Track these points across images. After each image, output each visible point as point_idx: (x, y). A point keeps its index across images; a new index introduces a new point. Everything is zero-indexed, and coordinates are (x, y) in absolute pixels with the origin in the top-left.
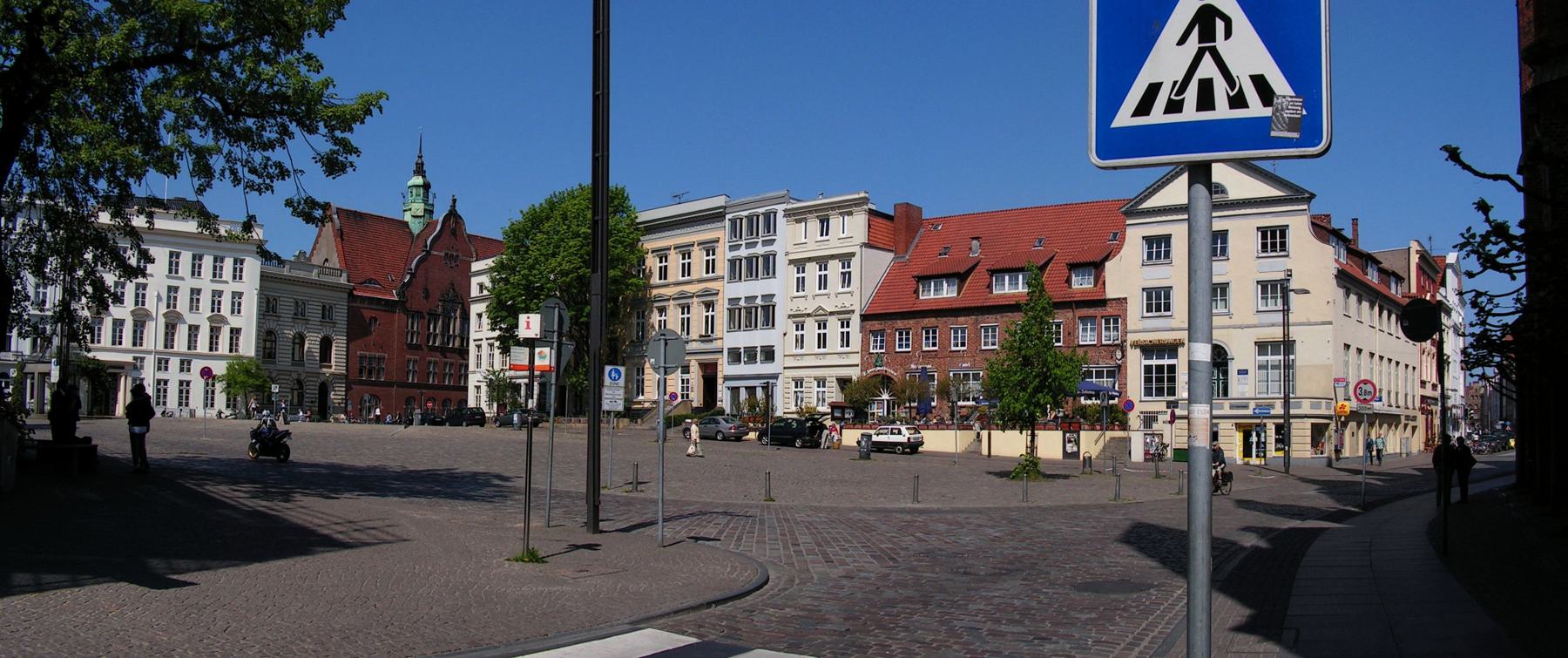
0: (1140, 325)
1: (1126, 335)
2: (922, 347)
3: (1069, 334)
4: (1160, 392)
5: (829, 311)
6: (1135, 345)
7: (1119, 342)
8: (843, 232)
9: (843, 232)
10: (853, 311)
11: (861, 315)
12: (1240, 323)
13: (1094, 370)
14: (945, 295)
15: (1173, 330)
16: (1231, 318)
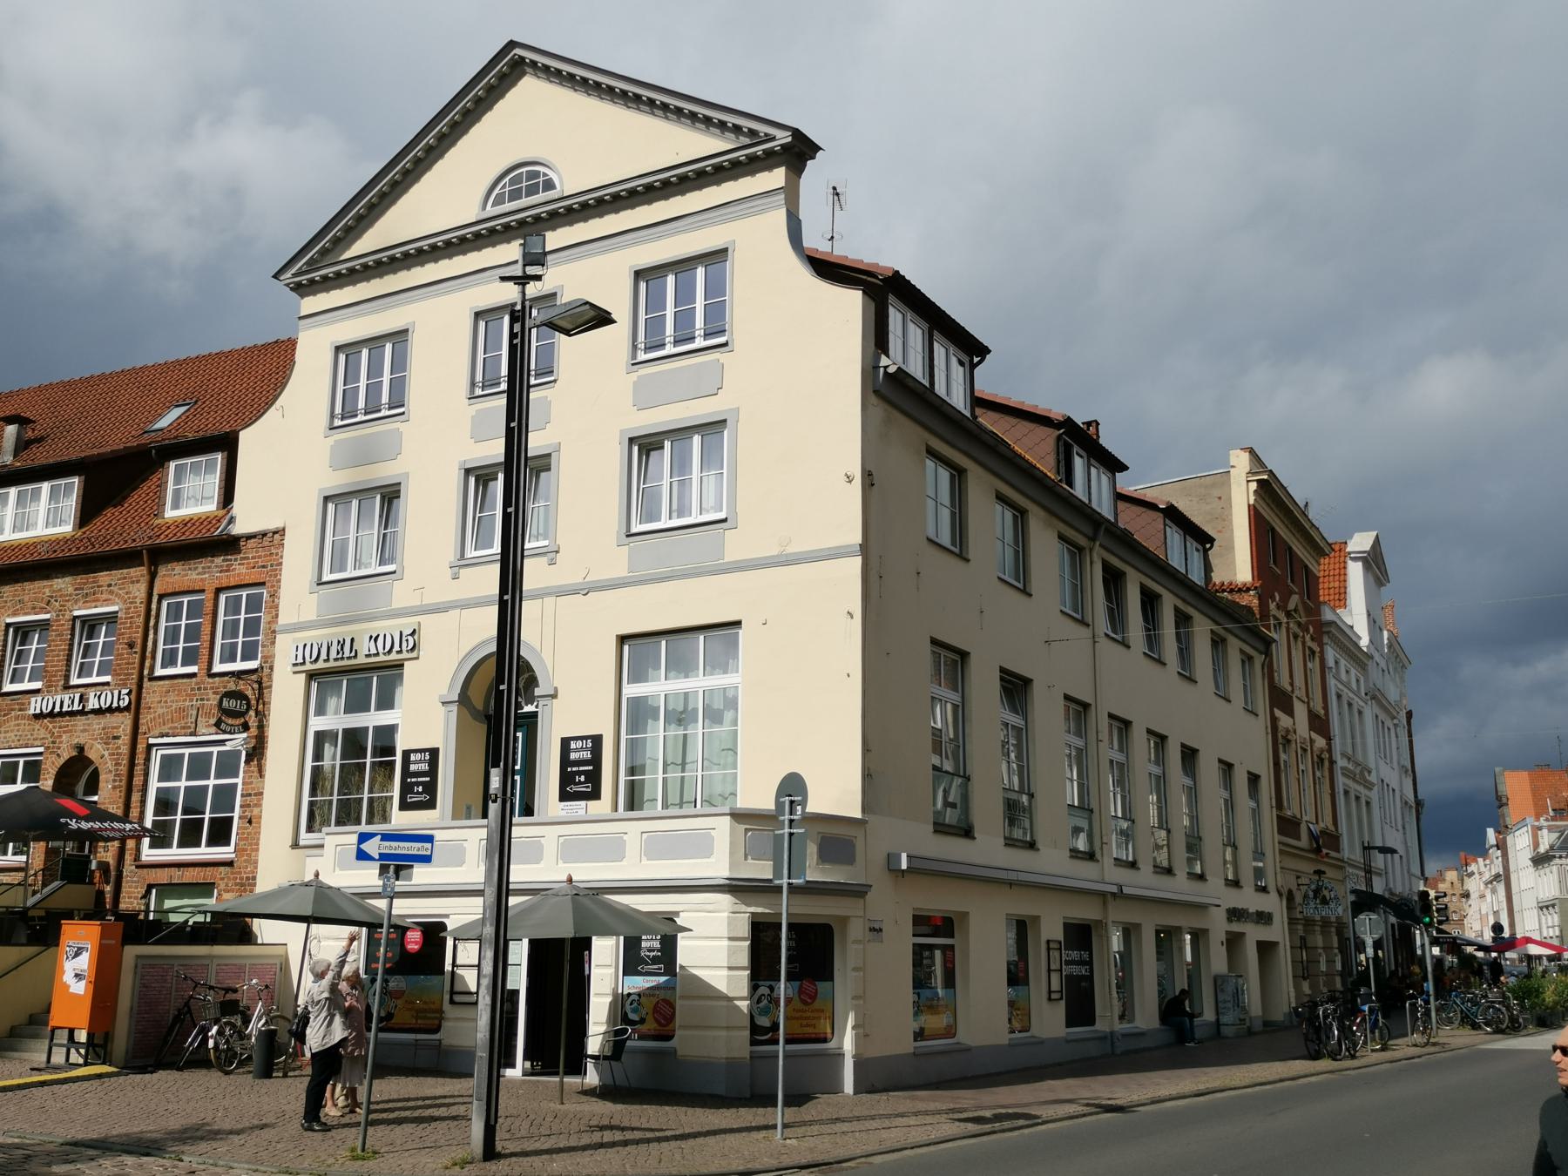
4: (347, 815)
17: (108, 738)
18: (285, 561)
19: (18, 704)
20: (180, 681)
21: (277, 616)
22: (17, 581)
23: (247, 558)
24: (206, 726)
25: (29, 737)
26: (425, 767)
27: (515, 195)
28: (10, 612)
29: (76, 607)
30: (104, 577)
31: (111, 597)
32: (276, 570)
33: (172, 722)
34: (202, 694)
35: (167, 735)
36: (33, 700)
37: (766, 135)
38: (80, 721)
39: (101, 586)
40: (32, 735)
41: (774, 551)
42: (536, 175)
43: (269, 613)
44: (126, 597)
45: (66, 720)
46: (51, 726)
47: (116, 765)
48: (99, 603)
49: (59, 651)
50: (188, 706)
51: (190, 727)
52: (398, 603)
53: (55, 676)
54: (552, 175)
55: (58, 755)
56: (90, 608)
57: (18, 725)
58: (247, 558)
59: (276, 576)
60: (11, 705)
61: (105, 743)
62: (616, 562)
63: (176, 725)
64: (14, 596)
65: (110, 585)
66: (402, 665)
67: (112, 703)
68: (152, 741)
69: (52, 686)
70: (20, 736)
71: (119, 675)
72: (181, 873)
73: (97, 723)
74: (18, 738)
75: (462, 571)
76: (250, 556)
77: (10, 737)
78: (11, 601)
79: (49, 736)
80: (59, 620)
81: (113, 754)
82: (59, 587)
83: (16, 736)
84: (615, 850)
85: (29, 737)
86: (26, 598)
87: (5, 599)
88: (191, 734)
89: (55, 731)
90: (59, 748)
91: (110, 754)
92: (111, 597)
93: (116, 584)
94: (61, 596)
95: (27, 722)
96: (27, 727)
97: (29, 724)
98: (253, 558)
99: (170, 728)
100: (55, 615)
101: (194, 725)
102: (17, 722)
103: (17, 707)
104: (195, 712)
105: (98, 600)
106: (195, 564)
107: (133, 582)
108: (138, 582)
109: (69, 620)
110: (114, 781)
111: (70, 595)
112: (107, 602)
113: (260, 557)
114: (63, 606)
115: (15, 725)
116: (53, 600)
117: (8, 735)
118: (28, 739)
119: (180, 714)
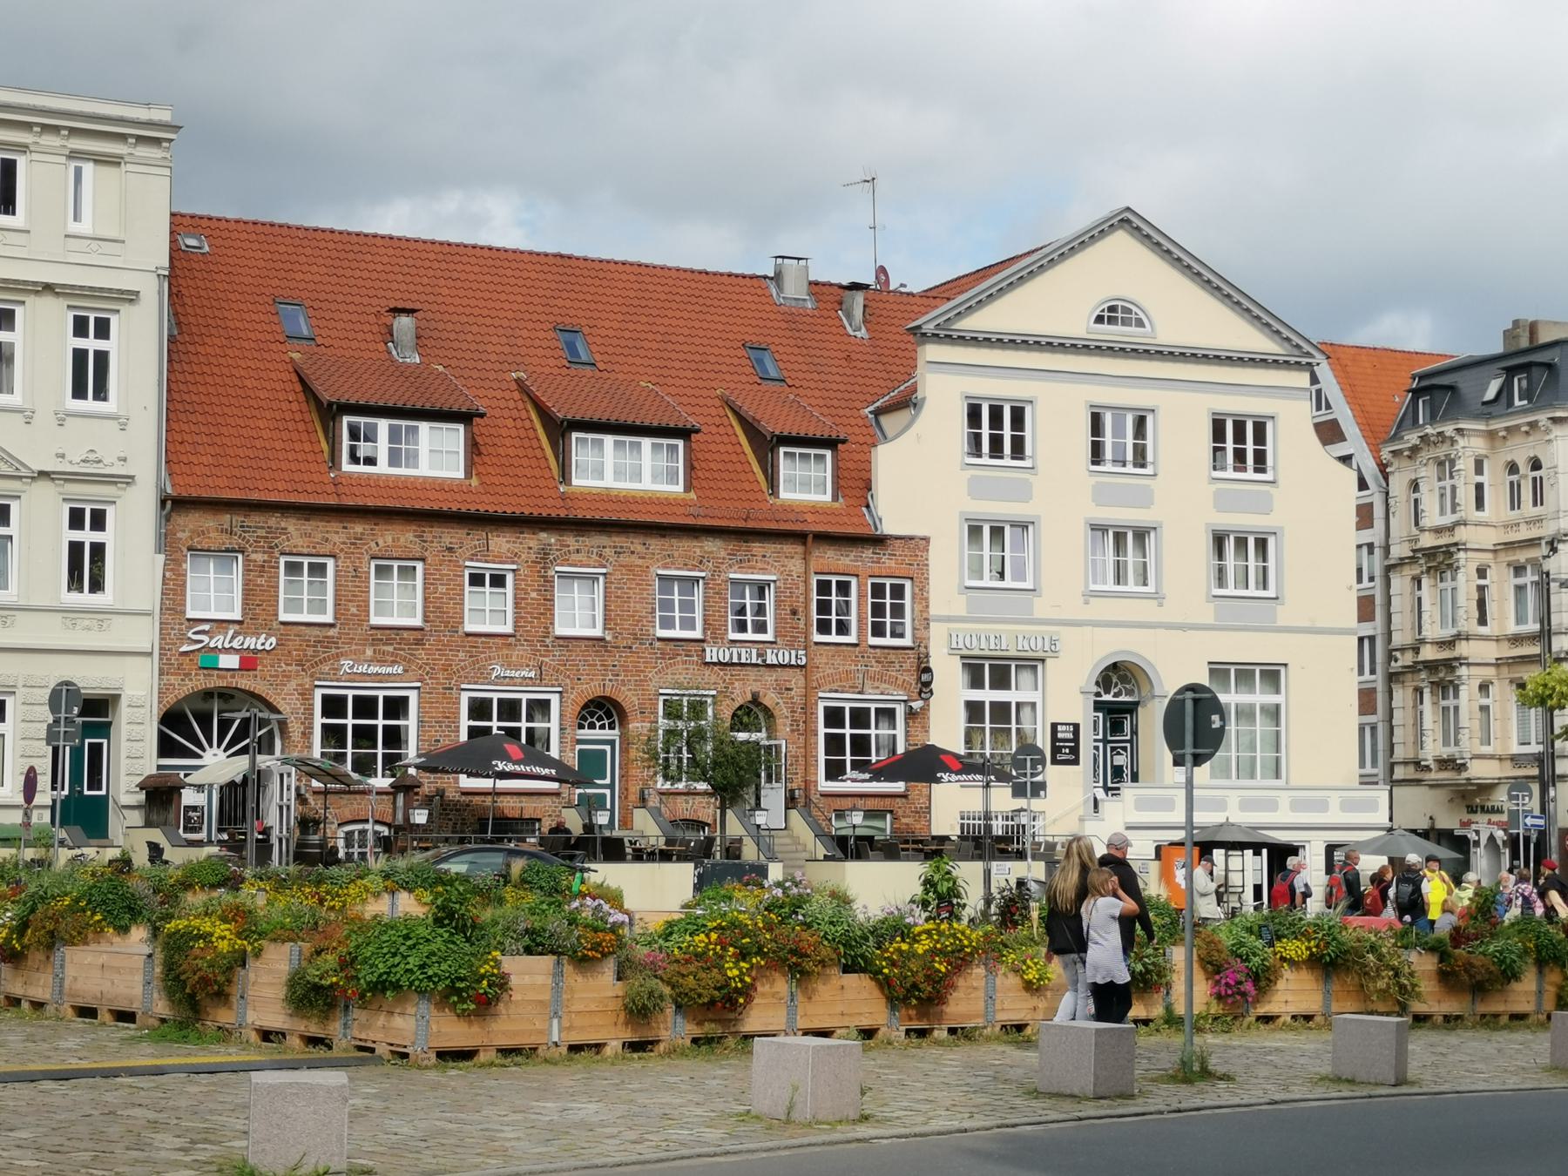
0: (959, 606)
1: (927, 627)
3: (794, 612)
5: (37, 467)
7: (907, 641)
8: (77, 218)
9: (77, 218)
10: (129, 480)
12: (1179, 620)
13: (873, 706)
16: (1161, 605)
18: (931, 562)
20: (845, 648)
21: (927, 606)
22: (664, 536)
26: (1070, 736)
27: (1112, 321)
30: (757, 548)
35: (836, 691)
36: (708, 650)
37: (1308, 353)
38: (752, 672)
41: (1307, 624)
42: (1130, 311)
45: (743, 672)
52: (1039, 613)
54: (1142, 316)
62: (1207, 615)
65: (764, 556)
66: (1043, 661)
68: (821, 695)
73: (770, 677)
75: (1091, 599)
84: (1272, 806)
86: (676, 554)
88: (859, 693)
89: (727, 678)
112: (763, 570)
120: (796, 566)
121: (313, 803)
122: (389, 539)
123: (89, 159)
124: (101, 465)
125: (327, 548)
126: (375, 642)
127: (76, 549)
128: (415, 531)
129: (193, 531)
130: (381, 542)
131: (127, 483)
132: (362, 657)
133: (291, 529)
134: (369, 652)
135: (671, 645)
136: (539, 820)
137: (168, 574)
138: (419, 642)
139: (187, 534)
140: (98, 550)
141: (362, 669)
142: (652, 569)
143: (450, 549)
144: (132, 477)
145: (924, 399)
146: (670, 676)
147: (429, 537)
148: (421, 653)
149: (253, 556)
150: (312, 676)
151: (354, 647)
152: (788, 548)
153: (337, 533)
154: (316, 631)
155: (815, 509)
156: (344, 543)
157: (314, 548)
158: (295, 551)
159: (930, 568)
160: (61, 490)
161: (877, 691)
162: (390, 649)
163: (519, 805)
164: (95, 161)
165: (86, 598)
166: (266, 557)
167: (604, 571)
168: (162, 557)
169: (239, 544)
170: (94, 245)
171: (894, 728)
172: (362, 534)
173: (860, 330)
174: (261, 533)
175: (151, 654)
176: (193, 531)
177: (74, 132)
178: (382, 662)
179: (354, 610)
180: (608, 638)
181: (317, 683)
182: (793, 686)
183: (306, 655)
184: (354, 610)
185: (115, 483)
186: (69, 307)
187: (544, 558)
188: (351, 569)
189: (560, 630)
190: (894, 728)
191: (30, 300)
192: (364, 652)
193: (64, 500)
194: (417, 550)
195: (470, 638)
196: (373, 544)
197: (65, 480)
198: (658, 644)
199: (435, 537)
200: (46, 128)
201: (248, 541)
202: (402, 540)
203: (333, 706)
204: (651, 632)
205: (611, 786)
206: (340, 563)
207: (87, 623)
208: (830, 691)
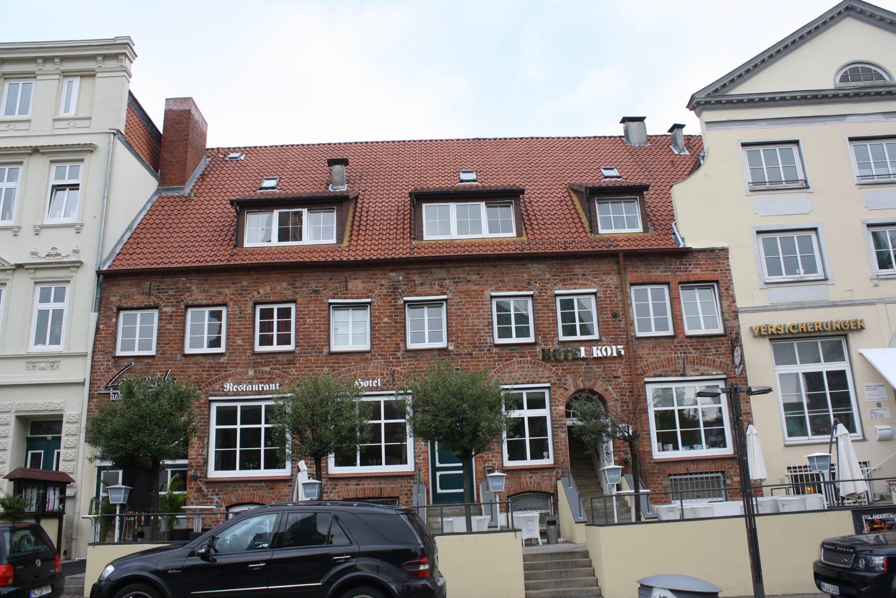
0: (764, 298)
1: (736, 317)
2: (252, 345)
3: (615, 316)
5: (13, 260)
6: (760, 334)
9: (67, 110)
11: (99, 273)
14: (308, 239)
15: (834, 305)
17: (609, 377)
18: (732, 267)
19: (518, 353)
21: (734, 302)
22: (495, 267)
23: (700, 264)
24: (693, 370)
25: (535, 376)
28: (493, 288)
29: (557, 288)
30: (578, 269)
31: (587, 283)
32: (726, 273)
33: (663, 367)
34: (684, 350)
35: (660, 376)
39: (576, 275)
40: (537, 375)
43: (727, 300)
44: (601, 283)
46: (554, 369)
47: (620, 395)
48: (577, 287)
49: (549, 317)
50: (674, 357)
51: (679, 371)
53: (549, 334)
55: (566, 389)
56: (569, 289)
57: (522, 367)
58: (700, 264)
59: (726, 277)
60: (510, 353)
61: (608, 381)
63: (667, 369)
64: (494, 277)
65: (584, 275)
67: (612, 353)
68: (647, 380)
69: (548, 341)
70: (526, 375)
71: (610, 335)
72: (695, 466)
74: (523, 376)
75: (881, 283)
76: (702, 263)
77: (515, 376)
78: (491, 280)
79: (554, 376)
80: (543, 296)
81: (617, 388)
82: (536, 273)
83: (521, 375)
85: (535, 376)
86: (507, 279)
87: (484, 279)
88: (681, 375)
90: (566, 384)
91: (613, 389)
92: (587, 283)
93: (589, 274)
94: (539, 280)
95: (530, 366)
96: (530, 369)
97: (532, 367)
98: (704, 264)
99: (663, 371)
100: (537, 292)
101: (683, 370)
102: (520, 365)
103: (518, 355)
104: (681, 361)
105: (576, 284)
106: (656, 265)
107: (603, 274)
108: (609, 274)
109: (552, 296)
110: (622, 406)
111: (549, 279)
112: (584, 286)
113: (709, 264)
114: (543, 286)
115: (519, 368)
116: (532, 282)
117: (513, 374)
118: (534, 378)
119: (668, 362)
120: (612, 280)
121: (205, 491)
122: (268, 288)
123: (76, 76)
124: (59, 257)
125: (220, 299)
126: (256, 365)
127: (43, 314)
128: (288, 281)
129: (122, 296)
130: (261, 291)
131: (79, 267)
132: (245, 377)
133: (194, 288)
134: (251, 373)
135: (507, 350)
136: (398, 498)
137: (101, 327)
138: (291, 362)
139: (117, 298)
140: (58, 314)
141: (243, 387)
142: (486, 293)
143: (316, 292)
144: (81, 263)
145: (709, 148)
146: (507, 375)
147: (299, 284)
148: (293, 371)
149: (165, 309)
150: (206, 393)
151: (239, 370)
152: (604, 266)
153: (228, 287)
154: (210, 360)
155: (628, 238)
156: (233, 294)
157: (210, 299)
158: (195, 303)
159: (733, 272)
160: (32, 276)
161: (697, 373)
162: (268, 369)
163: (377, 486)
164: (82, 76)
165: (48, 348)
166: (174, 309)
167: (445, 297)
168: (96, 314)
169: (154, 302)
170: (72, 123)
171: (720, 403)
172: (247, 286)
173: (684, 150)
174: (172, 292)
175: (83, 384)
176: (122, 296)
177: (63, 59)
178: (261, 380)
179: (240, 342)
180: (451, 348)
181: (210, 398)
182: (619, 373)
183: (201, 378)
184: (240, 342)
185: (68, 268)
186: (52, 162)
187: (394, 290)
188: (238, 312)
189: (411, 346)
190: (720, 403)
191: (25, 160)
192: (247, 372)
193: (36, 283)
194: (289, 294)
195: (333, 356)
196: (255, 293)
197: (36, 269)
198: (494, 350)
199: (305, 284)
200: (46, 60)
201: (162, 299)
202: (278, 288)
203: (226, 415)
204: (489, 340)
205: (435, 469)
206: (230, 309)
207: (43, 365)
208: (655, 376)
